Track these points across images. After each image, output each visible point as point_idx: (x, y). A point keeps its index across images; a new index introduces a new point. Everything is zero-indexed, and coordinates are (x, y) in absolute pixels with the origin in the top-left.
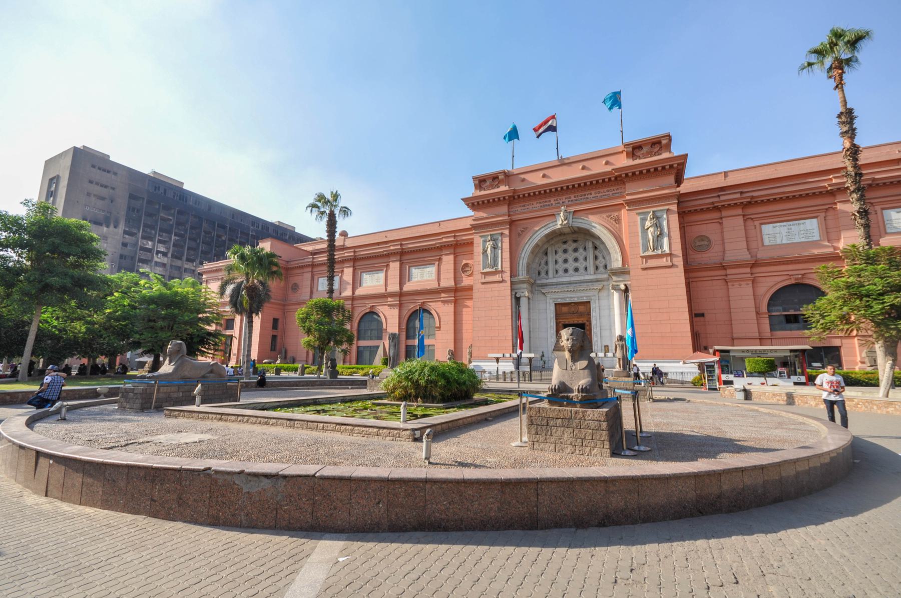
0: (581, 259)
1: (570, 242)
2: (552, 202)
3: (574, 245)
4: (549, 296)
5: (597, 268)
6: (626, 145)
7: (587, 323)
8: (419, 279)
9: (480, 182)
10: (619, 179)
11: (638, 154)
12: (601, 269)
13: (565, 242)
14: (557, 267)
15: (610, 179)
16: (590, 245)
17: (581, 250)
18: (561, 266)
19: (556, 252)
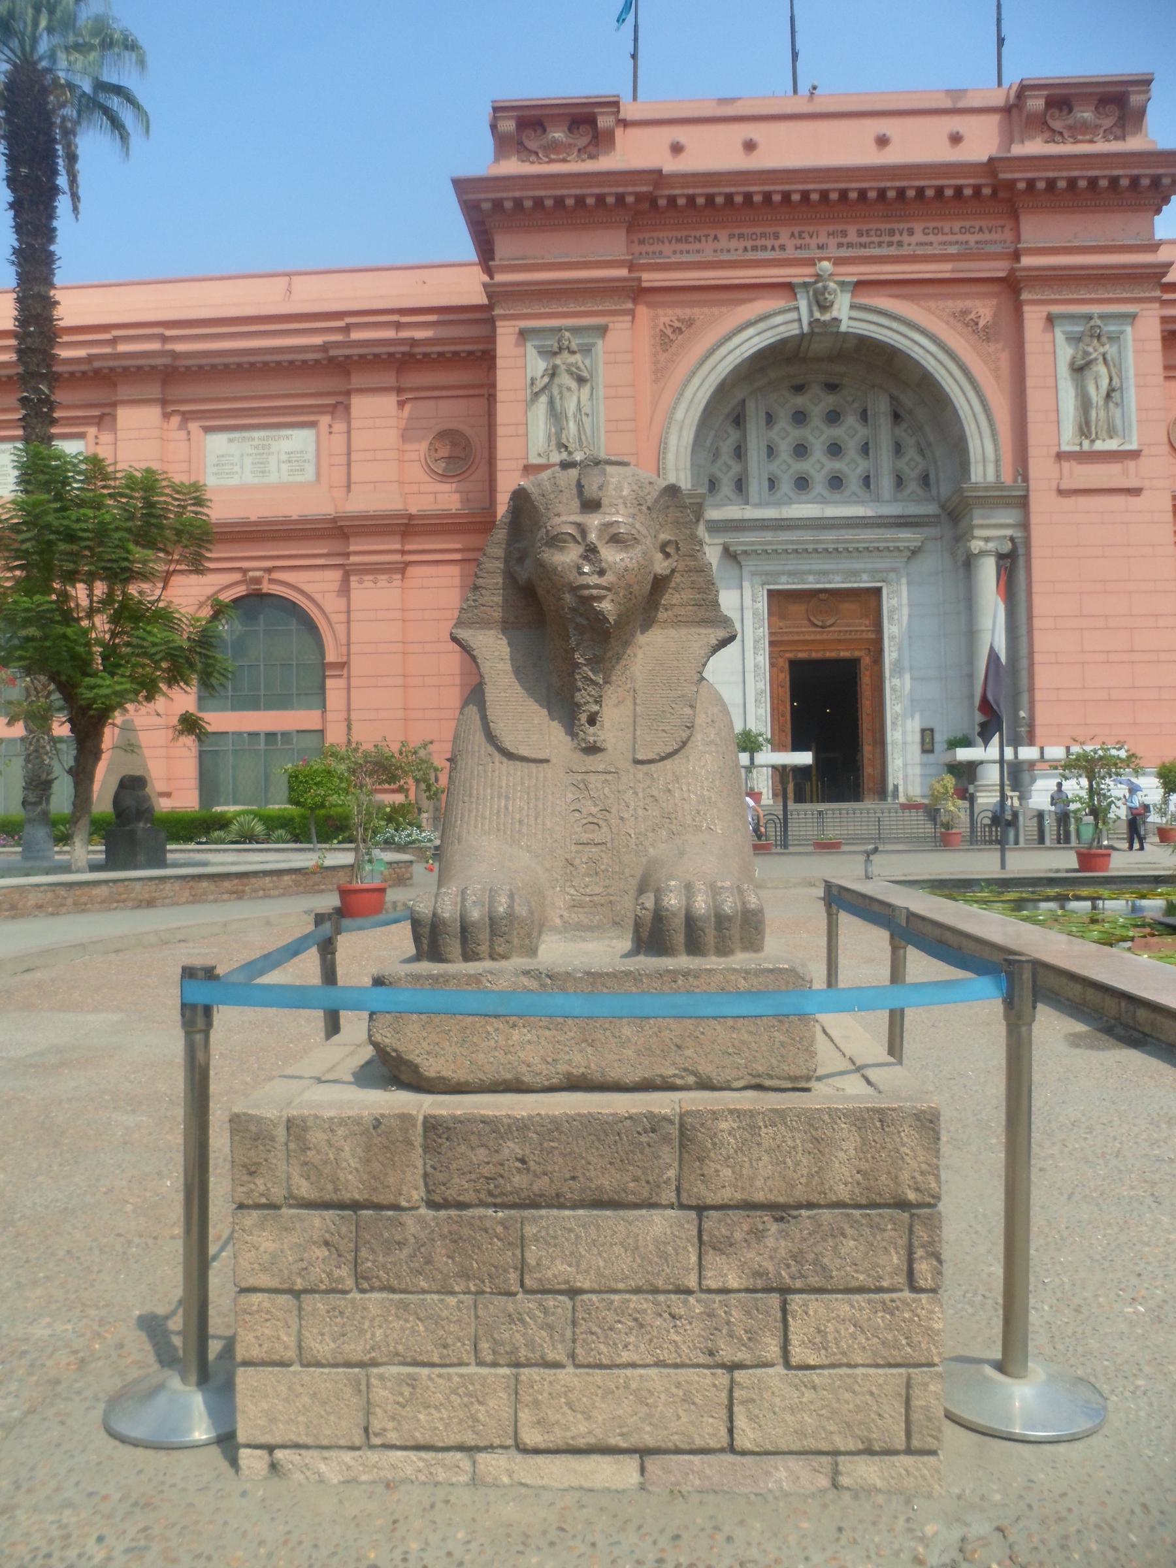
0: (852, 447)
1: (816, 390)
2: (784, 238)
3: (829, 401)
4: (749, 565)
5: (899, 481)
6: (1024, 90)
7: (866, 661)
8: (249, 478)
9: (524, 125)
10: (997, 194)
11: (1057, 125)
12: (913, 486)
13: (799, 389)
14: (774, 467)
15: (977, 189)
16: (881, 406)
17: (851, 420)
18: (787, 467)
19: (770, 419)
